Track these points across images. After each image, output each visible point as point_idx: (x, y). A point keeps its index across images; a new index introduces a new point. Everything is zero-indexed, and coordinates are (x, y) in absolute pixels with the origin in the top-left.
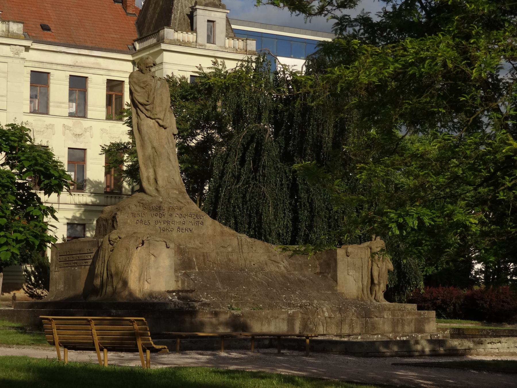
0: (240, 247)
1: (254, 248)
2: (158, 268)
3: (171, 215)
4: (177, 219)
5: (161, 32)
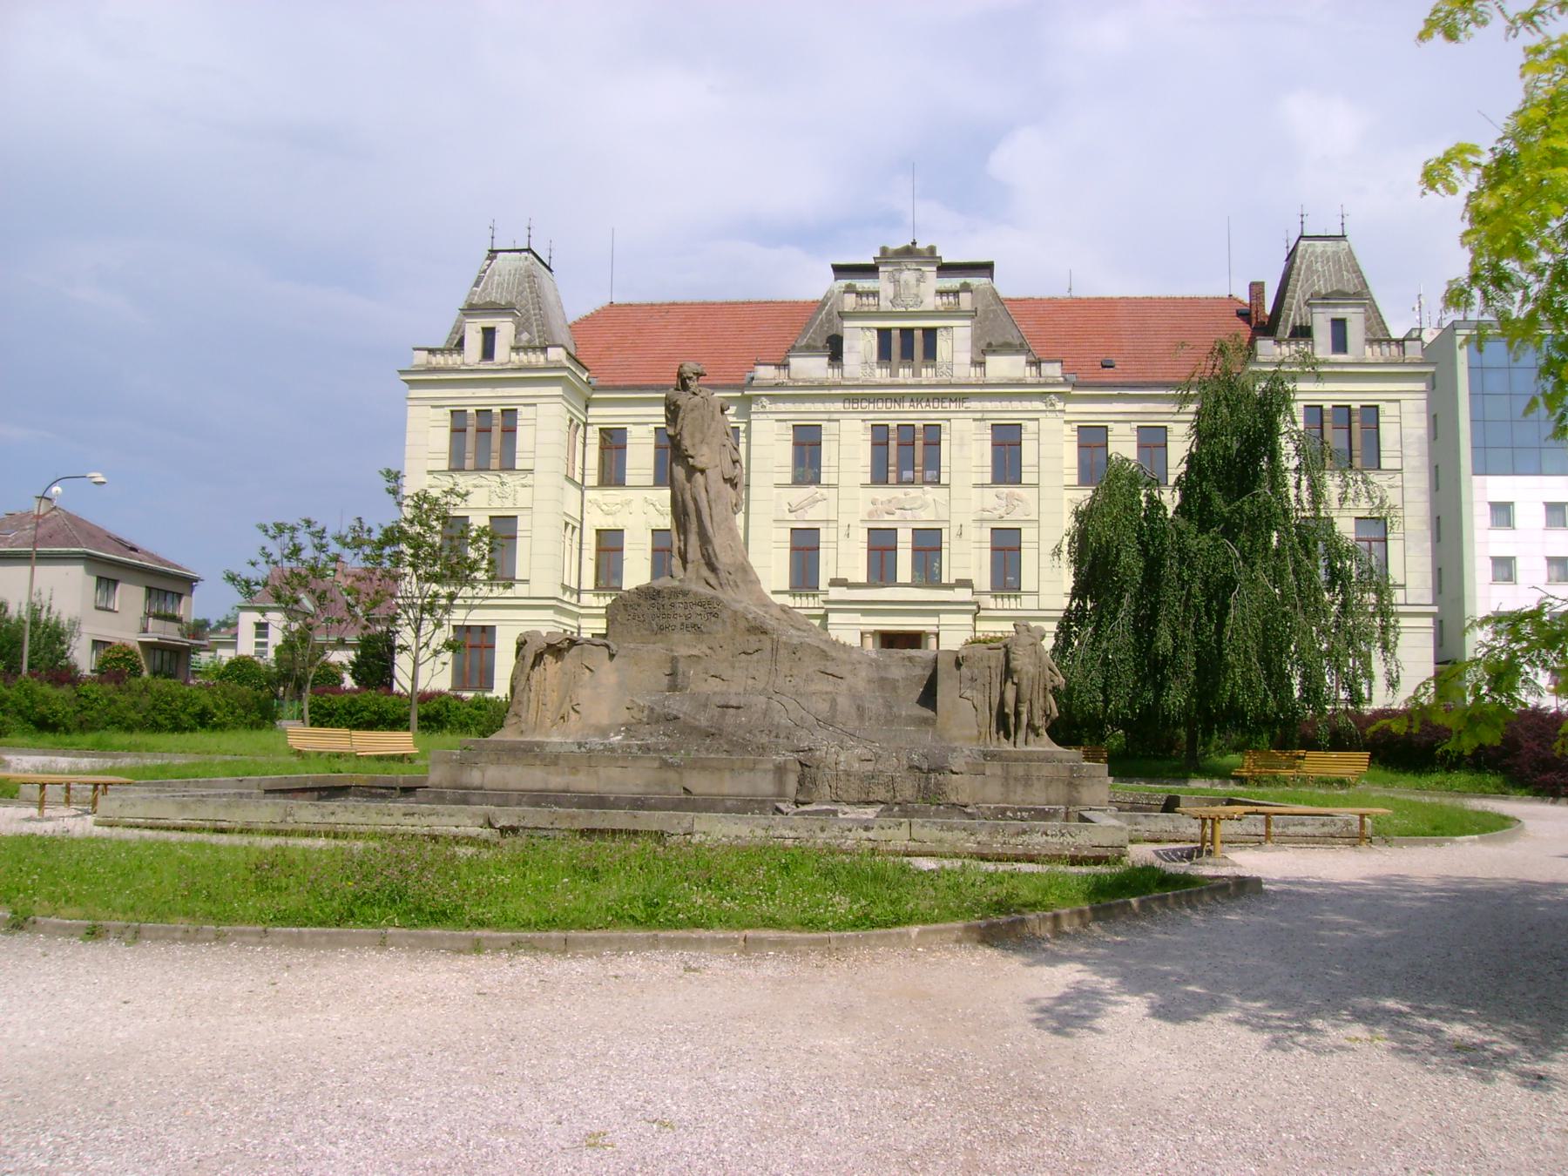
1: (799, 654)
3: (672, 605)
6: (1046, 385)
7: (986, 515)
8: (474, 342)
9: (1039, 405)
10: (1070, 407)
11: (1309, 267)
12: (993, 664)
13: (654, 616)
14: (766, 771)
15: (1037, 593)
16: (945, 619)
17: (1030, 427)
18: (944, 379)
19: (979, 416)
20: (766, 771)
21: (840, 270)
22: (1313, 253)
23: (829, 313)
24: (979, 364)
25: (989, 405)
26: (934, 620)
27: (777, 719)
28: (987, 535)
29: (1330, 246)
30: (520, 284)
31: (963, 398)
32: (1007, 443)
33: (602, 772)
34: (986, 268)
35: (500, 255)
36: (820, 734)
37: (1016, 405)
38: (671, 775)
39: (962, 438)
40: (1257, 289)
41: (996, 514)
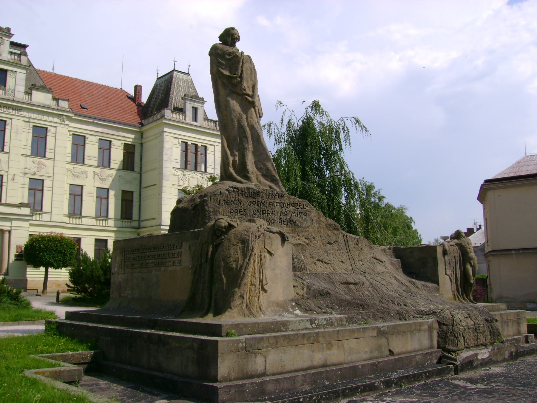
0: (347, 244)
1: (360, 245)
3: (271, 204)
4: (278, 209)
5: (163, 111)
6: (61, 110)
7: (27, 171)
9: (57, 120)
10: (72, 124)
11: (178, 83)
12: (456, 255)
14: (425, 331)
15: (50, 213)
16: (15, 223)
17: (51, 130)
18: (10, 97)
19: (27, 120)
20: (425, 331)
22: (179, 78)
24: (29, 93)
25: (32, 115)
26: (9, 224)
28: (27, 181)
29: (185, 77)
31: (19, 109)
32: (40, 135)
33: (345, 342)
37: (46, 118)
38: (383, 341)
39: (17, 129)
40: (138, 89)
41: (32, 171)
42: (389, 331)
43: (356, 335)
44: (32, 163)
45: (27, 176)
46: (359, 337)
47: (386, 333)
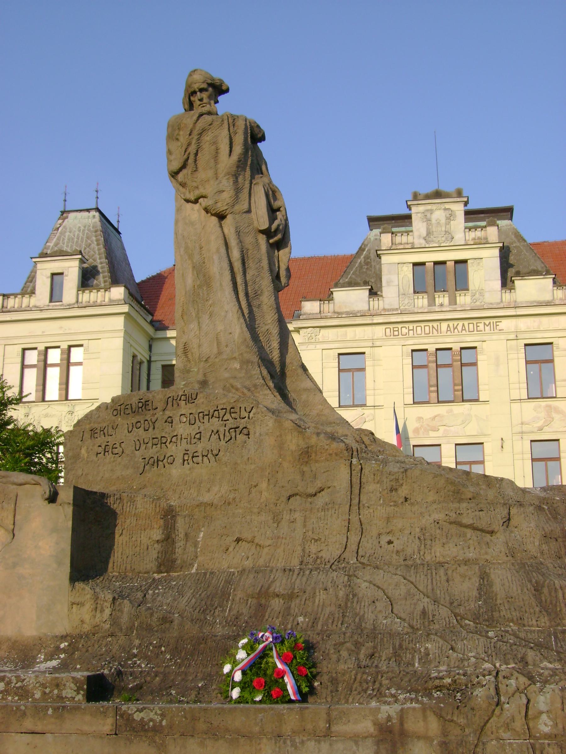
0: (356, 491)
1: (404, 491)
2: (15, 565)
3: (170, 421)
4: (183, 429)
7: (525, 428)
8: (43, 285)
13: (139, 444)
20: (356, 739)
21: (373, 221)
23: (367, 257)
27: (370, 616)
30: (88, 238)
34: (507, 212)
35: (72, 215)
36: (472, 649)
42: (171, 726)
43: (28, 724)
44: (532, 411)
45: (525, 437)
46: (39, 728)
47: (157, 729)
